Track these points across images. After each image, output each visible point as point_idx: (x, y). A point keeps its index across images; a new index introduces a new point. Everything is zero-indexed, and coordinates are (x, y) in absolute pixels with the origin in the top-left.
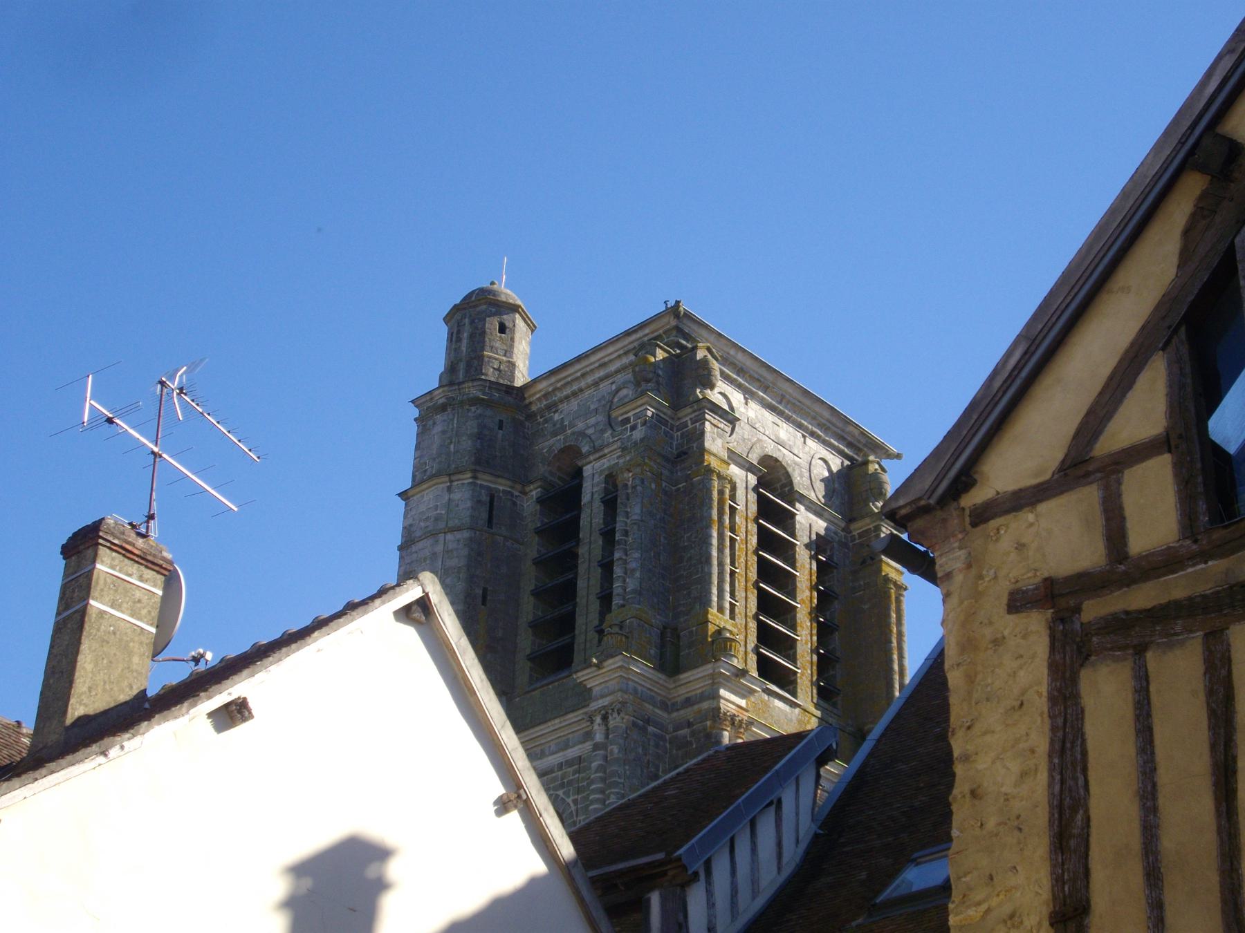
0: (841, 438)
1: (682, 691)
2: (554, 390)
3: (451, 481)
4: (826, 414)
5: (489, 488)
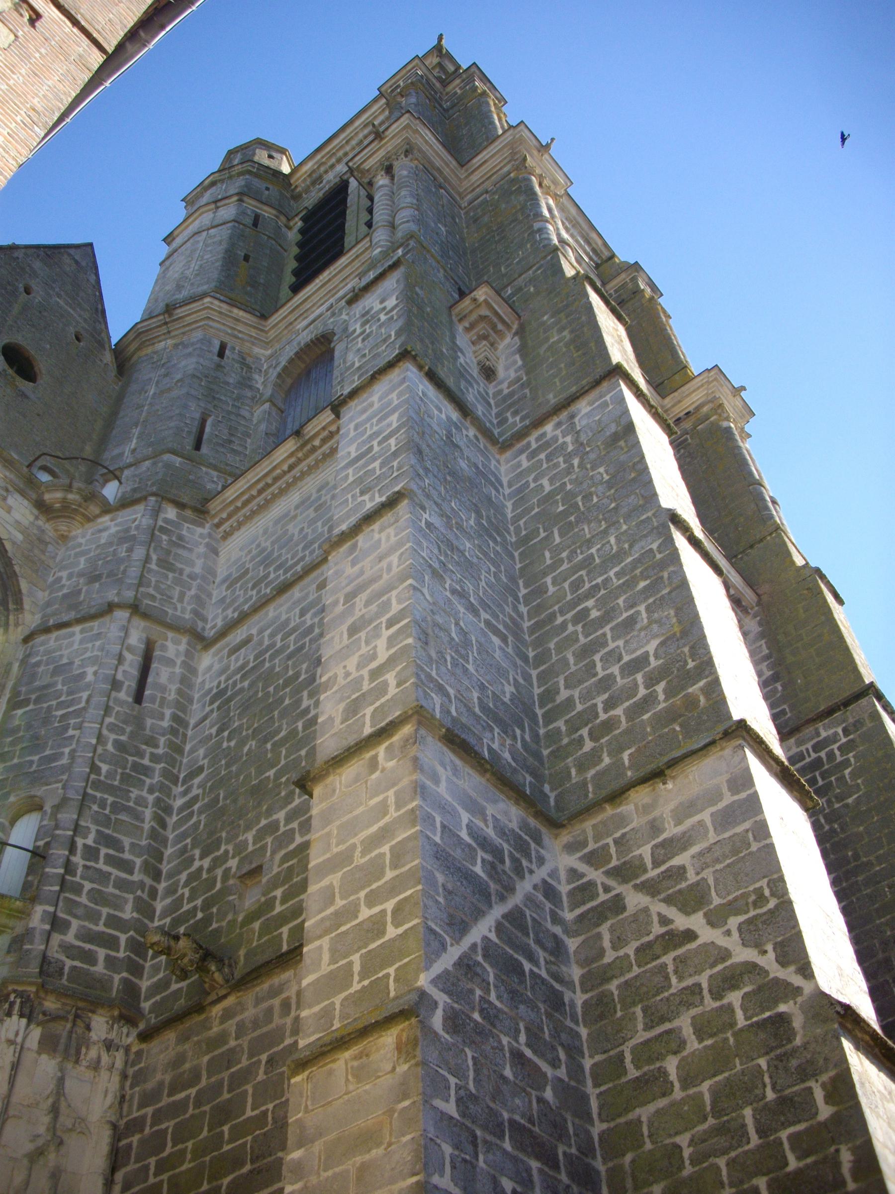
0: (588, 242)
1: (474, 178)
2: (318, 168)
3: (217, 208)
4: (573, 211)
5: (253, 211)
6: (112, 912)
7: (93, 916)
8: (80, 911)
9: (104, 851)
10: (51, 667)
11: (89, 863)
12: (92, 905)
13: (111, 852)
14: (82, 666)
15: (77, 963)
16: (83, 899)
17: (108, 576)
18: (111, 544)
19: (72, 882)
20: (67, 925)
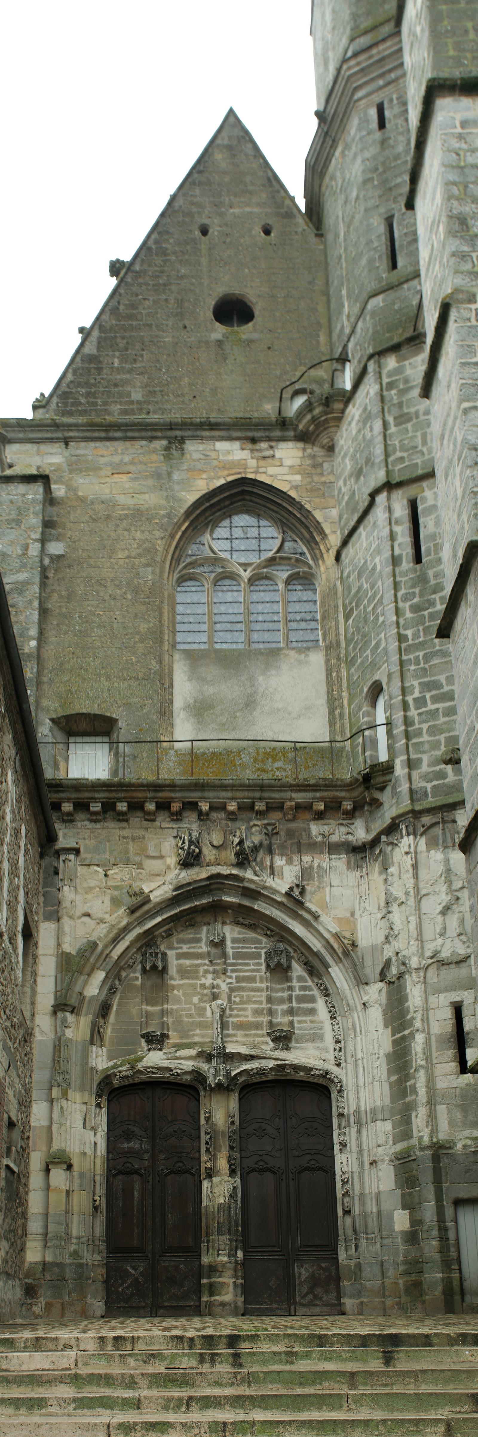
6: (447, 735)
7: (435, 745)
8: (426, 747)
9: (428, 696)
10: (356, 573)
11: (420, 711)
12: (432, 738)
13: (434, 692)
14: (372, 561)
15: (435, 783)
16: (425, 738)
17: (366, 464)
18: (359, 431)
19: (414, 730)
20: (420, 761)
